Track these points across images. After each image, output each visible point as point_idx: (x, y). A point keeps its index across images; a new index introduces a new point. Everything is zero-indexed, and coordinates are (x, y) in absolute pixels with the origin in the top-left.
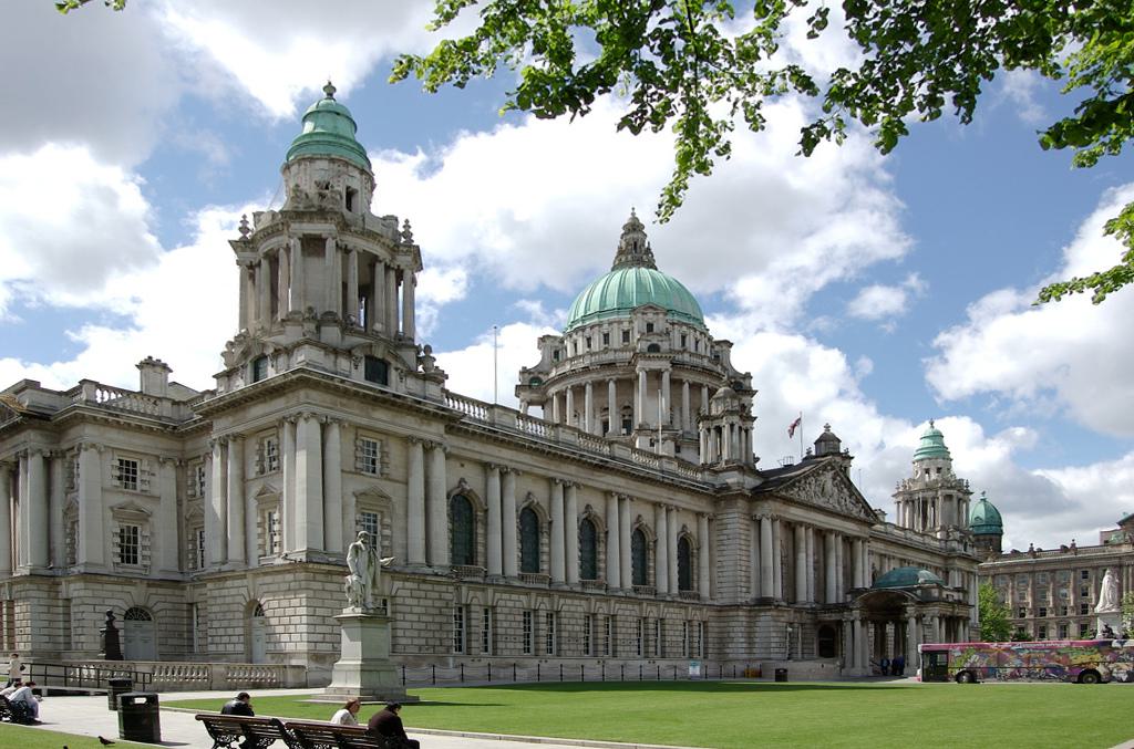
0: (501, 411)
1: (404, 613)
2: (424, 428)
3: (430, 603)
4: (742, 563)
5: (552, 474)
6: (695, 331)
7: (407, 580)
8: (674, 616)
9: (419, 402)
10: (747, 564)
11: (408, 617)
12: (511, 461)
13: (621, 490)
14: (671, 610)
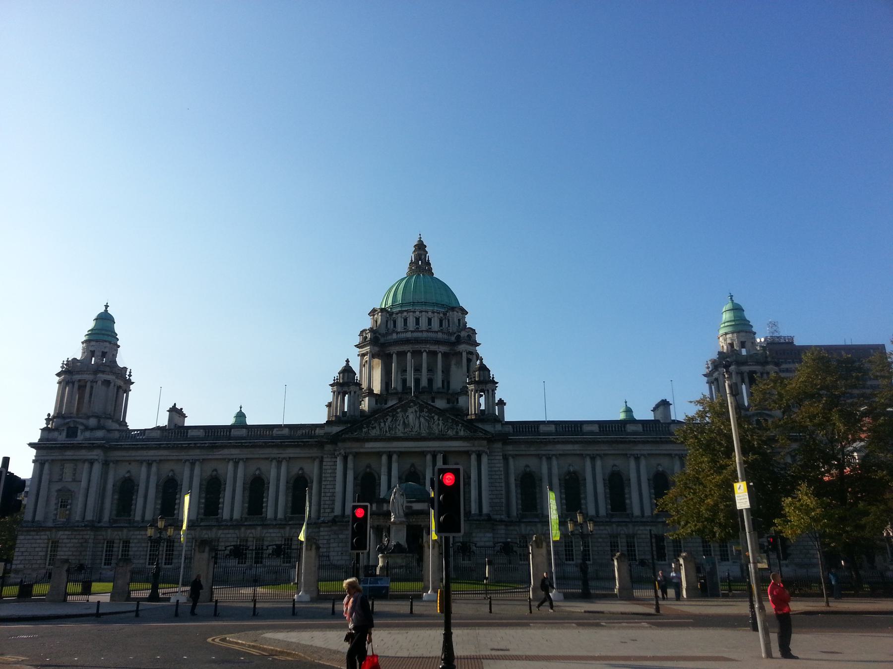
0: (149, 431)
1: (62, 547)
2: (89, 454)
3: (76, 541)
4: (328, 491)
5: (180, 458)
6: (414, 312)
7: (66, 530)
8: (273, 535)
9: (80, 444)
10: (331, 491)
11: (65, 549)
12: (152, 456)
13: (234, 457)
14: (271, 531)
